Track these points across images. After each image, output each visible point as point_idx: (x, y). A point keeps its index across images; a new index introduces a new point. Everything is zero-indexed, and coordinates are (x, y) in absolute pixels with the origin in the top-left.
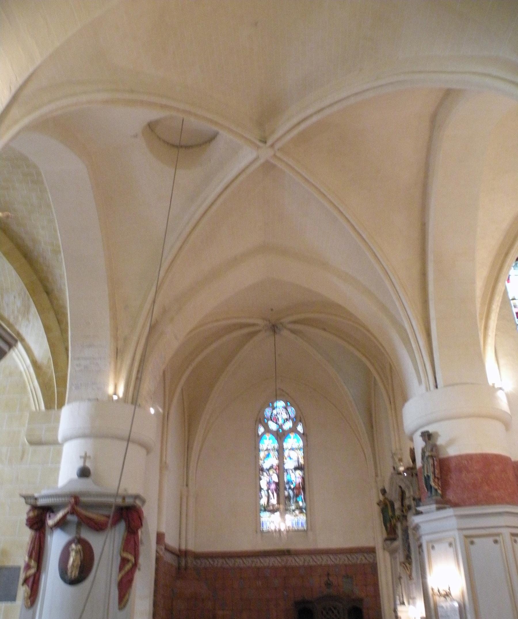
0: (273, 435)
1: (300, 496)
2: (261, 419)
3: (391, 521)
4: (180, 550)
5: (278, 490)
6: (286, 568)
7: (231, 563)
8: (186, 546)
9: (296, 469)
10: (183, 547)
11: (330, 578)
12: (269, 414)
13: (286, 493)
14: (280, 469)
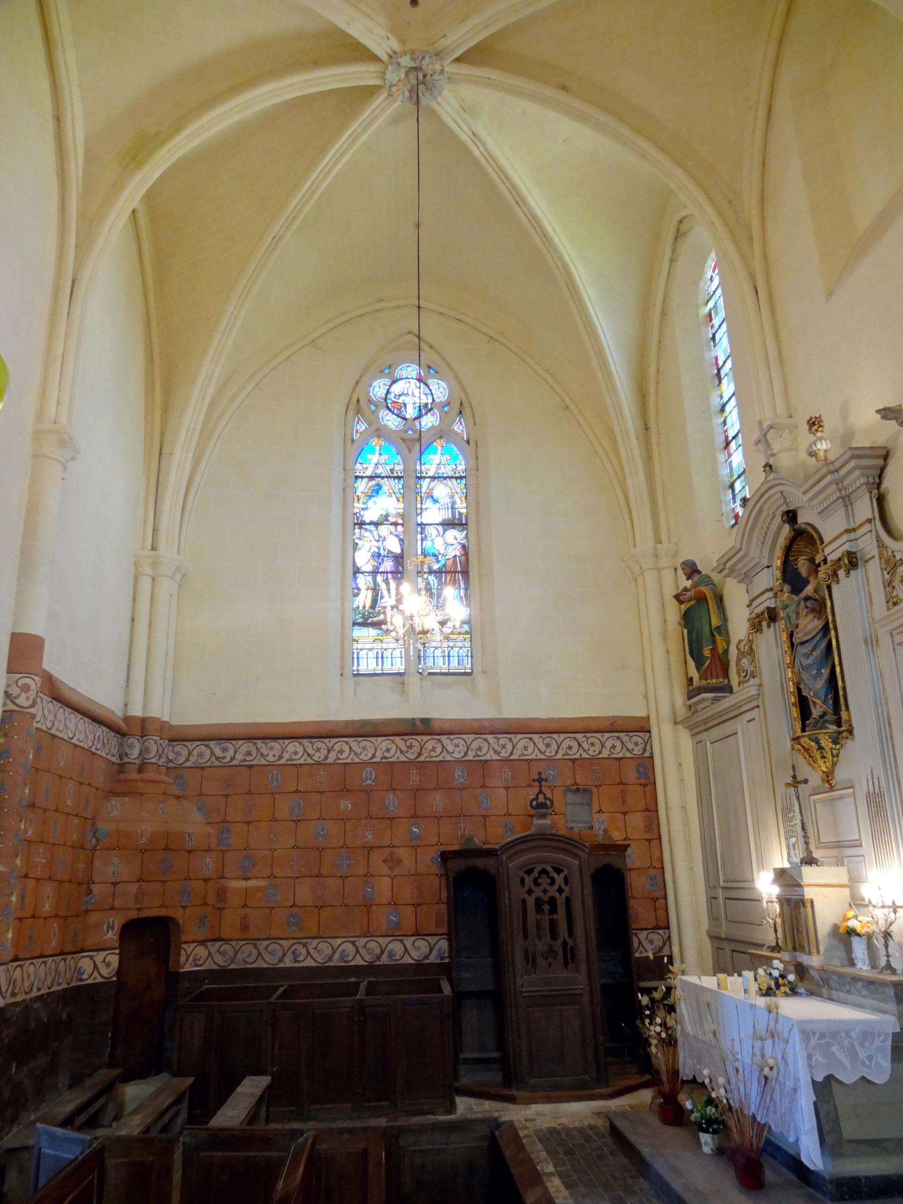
0: (393, 443)
3: (714, 642)
4: (127, 719)
6: (421, 766)
7: (271, 752)
8: (144, 708)
9: (448, 524)
10: (137, 711)
12: (381, 393)
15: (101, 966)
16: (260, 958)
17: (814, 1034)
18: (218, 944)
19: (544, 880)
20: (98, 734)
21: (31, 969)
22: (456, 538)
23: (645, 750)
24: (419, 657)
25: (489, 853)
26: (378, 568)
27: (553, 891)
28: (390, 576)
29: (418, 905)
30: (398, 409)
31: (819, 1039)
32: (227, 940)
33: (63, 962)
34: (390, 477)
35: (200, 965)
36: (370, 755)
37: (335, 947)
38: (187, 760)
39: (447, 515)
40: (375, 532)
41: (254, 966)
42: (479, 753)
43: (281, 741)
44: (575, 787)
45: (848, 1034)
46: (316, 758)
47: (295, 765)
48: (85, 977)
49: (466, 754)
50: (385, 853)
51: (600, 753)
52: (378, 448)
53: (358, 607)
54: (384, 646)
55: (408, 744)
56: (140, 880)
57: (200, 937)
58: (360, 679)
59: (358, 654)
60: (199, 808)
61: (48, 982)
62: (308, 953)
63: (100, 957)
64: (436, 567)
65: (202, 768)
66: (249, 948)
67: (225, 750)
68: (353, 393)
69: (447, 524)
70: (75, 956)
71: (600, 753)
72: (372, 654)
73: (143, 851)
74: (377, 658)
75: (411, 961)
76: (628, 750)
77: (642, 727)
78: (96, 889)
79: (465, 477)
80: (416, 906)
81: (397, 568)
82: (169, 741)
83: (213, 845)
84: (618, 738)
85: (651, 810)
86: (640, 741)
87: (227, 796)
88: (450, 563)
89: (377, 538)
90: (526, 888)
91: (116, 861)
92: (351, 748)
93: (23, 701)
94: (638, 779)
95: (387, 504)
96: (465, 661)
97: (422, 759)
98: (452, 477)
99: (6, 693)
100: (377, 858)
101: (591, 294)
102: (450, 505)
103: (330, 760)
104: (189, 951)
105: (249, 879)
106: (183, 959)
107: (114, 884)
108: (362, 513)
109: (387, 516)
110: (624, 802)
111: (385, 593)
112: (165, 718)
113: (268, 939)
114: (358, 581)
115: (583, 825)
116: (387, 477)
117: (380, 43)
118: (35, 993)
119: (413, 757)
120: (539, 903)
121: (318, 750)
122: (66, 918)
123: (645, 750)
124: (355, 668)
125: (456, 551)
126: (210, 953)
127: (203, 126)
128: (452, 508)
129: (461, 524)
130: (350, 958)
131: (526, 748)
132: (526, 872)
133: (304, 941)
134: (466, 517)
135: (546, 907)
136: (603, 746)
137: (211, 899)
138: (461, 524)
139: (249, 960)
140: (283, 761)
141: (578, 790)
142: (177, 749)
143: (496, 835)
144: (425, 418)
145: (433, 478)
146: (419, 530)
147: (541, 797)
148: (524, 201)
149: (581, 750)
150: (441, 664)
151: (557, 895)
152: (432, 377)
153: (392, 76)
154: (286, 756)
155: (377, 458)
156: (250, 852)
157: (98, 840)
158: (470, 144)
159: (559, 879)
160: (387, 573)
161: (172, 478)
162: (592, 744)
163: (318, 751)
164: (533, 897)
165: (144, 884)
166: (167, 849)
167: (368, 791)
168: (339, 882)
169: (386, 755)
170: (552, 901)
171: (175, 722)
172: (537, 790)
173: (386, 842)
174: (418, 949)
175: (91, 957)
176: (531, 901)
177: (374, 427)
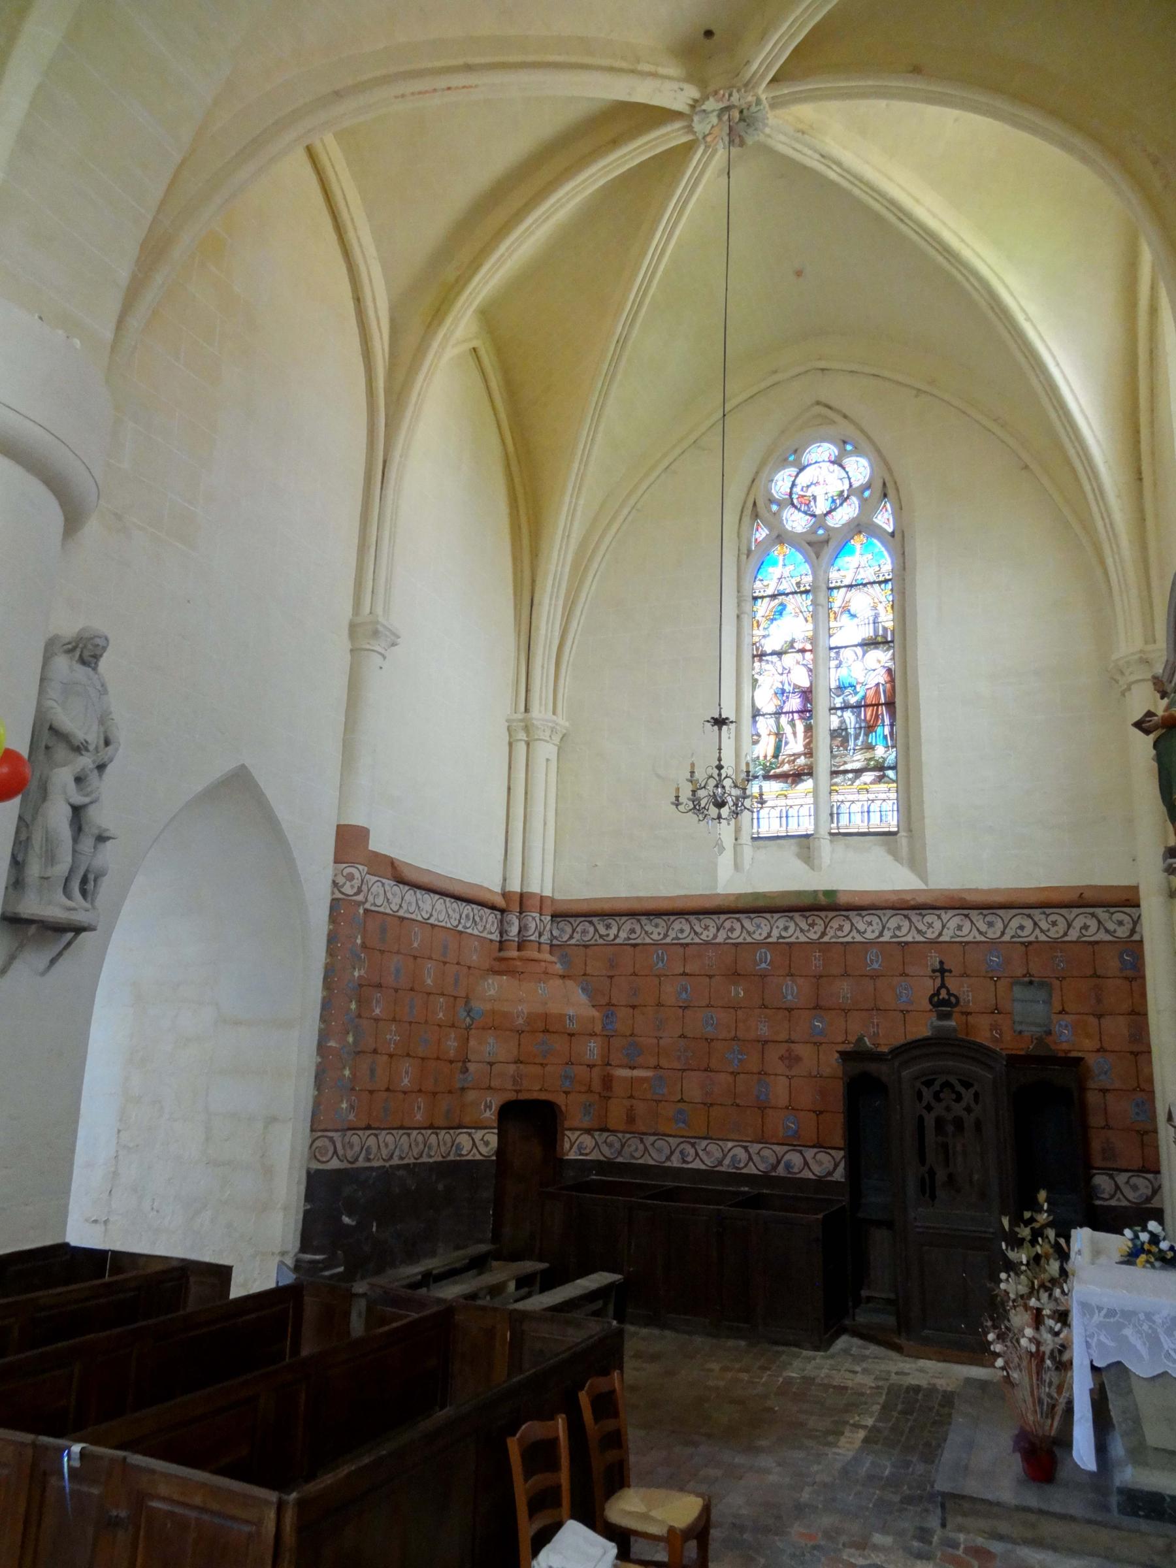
1: (879, 730)
2: (760, 504)
4: (505, 895)
5: (806, 712)
9: (870, 644)
10: (515, 886)
11: (952, 984)
13: (835, 722)
14: (817, 648)
15: (480, 1144)
16: (647, 1154)
17: (1100, 1309)
18: (605, 1134)
19: (946, 1094)
20: (465, 912)
21: (389, 1139)
22: (879, 661)
23: (1133, 931)
24: (831, 815)
25: (877, 1057)
26: (782, 708)
27: (958, 1109)
28: (796, 716)
29: (821, 1112)
30: (804, 505)
31: (1106, 1316)
32: (613, 1132)
33: (434, 1136)
34: (796, 593)
35: (586, 1155)
36: (765, 934)
37: (726, 1150)
38: (571, 937)
39: (868, 632)
40: (778, 664)
41: (640, 1161)
42: (897, 933)
43: (665, 918)
44: (1026, 979)
45: (1149, 1316)
46: (704, 937)
47: (682, 945)
48: (464, 1152)
49: (881, 935)
50: (782, 1049)
51: (1065, 934)
52: (781, 558)
54: (789, 802)
55: (810, 921)
56: (518, 1061)
57: (586, 1124)
58: (761, 843)
60: (583, 989)
61: (415, 1152)
62: (697, 1154)
63: (478, 1135)
64: (853, 700)
65: (586, 946)
66: (634, 1143)
67: (608, 927)
68: (748, 494)
69: (866, 645)
70: (452, 1131)
71: (1065, 934)
72: (776, 813)
73: (520, 1032)
75: (811, 1176)
76: (1107, 931)
77: (1128, 900)
78: (472, 1067)
80: (819, 1113)
81: (805, 706)
82: (552, 916)
83: (598, 1029)
84: (1093, 915)
85: (1138, 1014)
86: (1126, 919)
87: (611, 977)
88: (871, 693)
90: (924, 1103)
91: (491, 1040)
92: (743, 927)
93: (348, 889)
94: (1121, 970)
95: (793, 626)
96: (890, 818)
97: (826, 939)
98: (874, 582)
99: (334, 882)
100: (773, 1054)
101: (1032, 309)
102: (871, 619)
103: (720, 940)
104: (573, 1138)
105: (634, 1068)
106: (567, 1145)
107: (491, 1064)
108: (763, 641)
109: (793, 641)
110: (1099, 1001)
112: (547, 892)
113: (654, 1134)
114: (758, 725)
115: (1038, 1029)
116: (792, 593)
117: (673, 94)
118: (395, 1161)
119: (815, 937)
120: (940, 1123)
121: (706, 928)
122: (435, 1094)
123: (1133, 931)
124: (755, 830)
125: (881, 677)
126: (597, 1143)
127: (502, 255)
129: (887, 642)
130: (742, 1165)
131: (960, 928)
132: (923, 1083)
133: (693, 1141)
134: (893, 632)
135: (950, 1128)
136: (1069, 926)
137: (597, 1085)
138: (887, 642)
139: (637, 1155)
140: (668, 940)
141: (1031, 983)
142: (562, 925)
143: (886, 1035)
144: (839, 510)
146: (833, 654)
147: (943, 992)
148: (909, 216)
149: (1038, 930)
150: (858, 822)
151: (964, 1114)
152: (850, 454)
153: (700, 127)
154: (672, 934)
155: (784, 569)
156: (636, 1038)
157: (472, 1019)
158: (821, 168)
159: (968, 1095)
160: (793, 712)
161: (543, 631)
162: (1054, 924)
163: (708, 931)
164: (933, 1115)
165: (522, 1066)
166: (546, 1031)
167: (763, 976)
168: (730, 1079)
169: (784, 934)
170: (959, 1124)
171: (558, 896)
172: (938, 982)
173: (783, 1036)
174: (820, 1163)
175: (470, 1134)
176: (930, 1120)
177: (775, 534)
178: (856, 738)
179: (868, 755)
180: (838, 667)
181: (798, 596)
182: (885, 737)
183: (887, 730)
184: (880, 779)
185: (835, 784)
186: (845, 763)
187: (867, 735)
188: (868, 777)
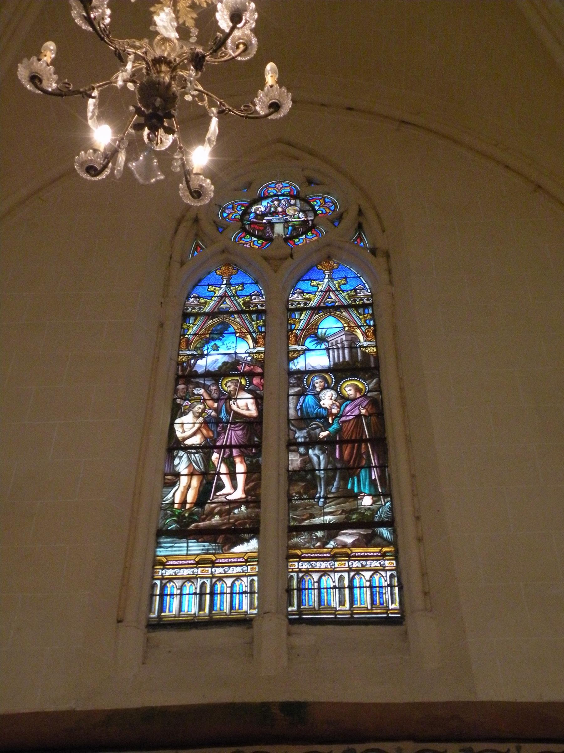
24: (289, 591)
26: (215, 441)
30: (263, 231)
53: (173, 503)
59: (163, 587)
69: (340, 370)
74: (202, 594)
79: (371, 305)
81: (250, 439)
89: (215, 396)
96: (387, 597)
111: (225, 479)
128: (351, 348)
145: (316, 309)
160: (231, 447)
178: (329, 482)
179: (347, 506)
180: (298, 395)
181: (246, 317)
182: (373, 483)
183: (374, 475)
184: (367, 541)
185: (296, 546)
186: (312, 516)
187: (344, 479)
188: (347, 538)
